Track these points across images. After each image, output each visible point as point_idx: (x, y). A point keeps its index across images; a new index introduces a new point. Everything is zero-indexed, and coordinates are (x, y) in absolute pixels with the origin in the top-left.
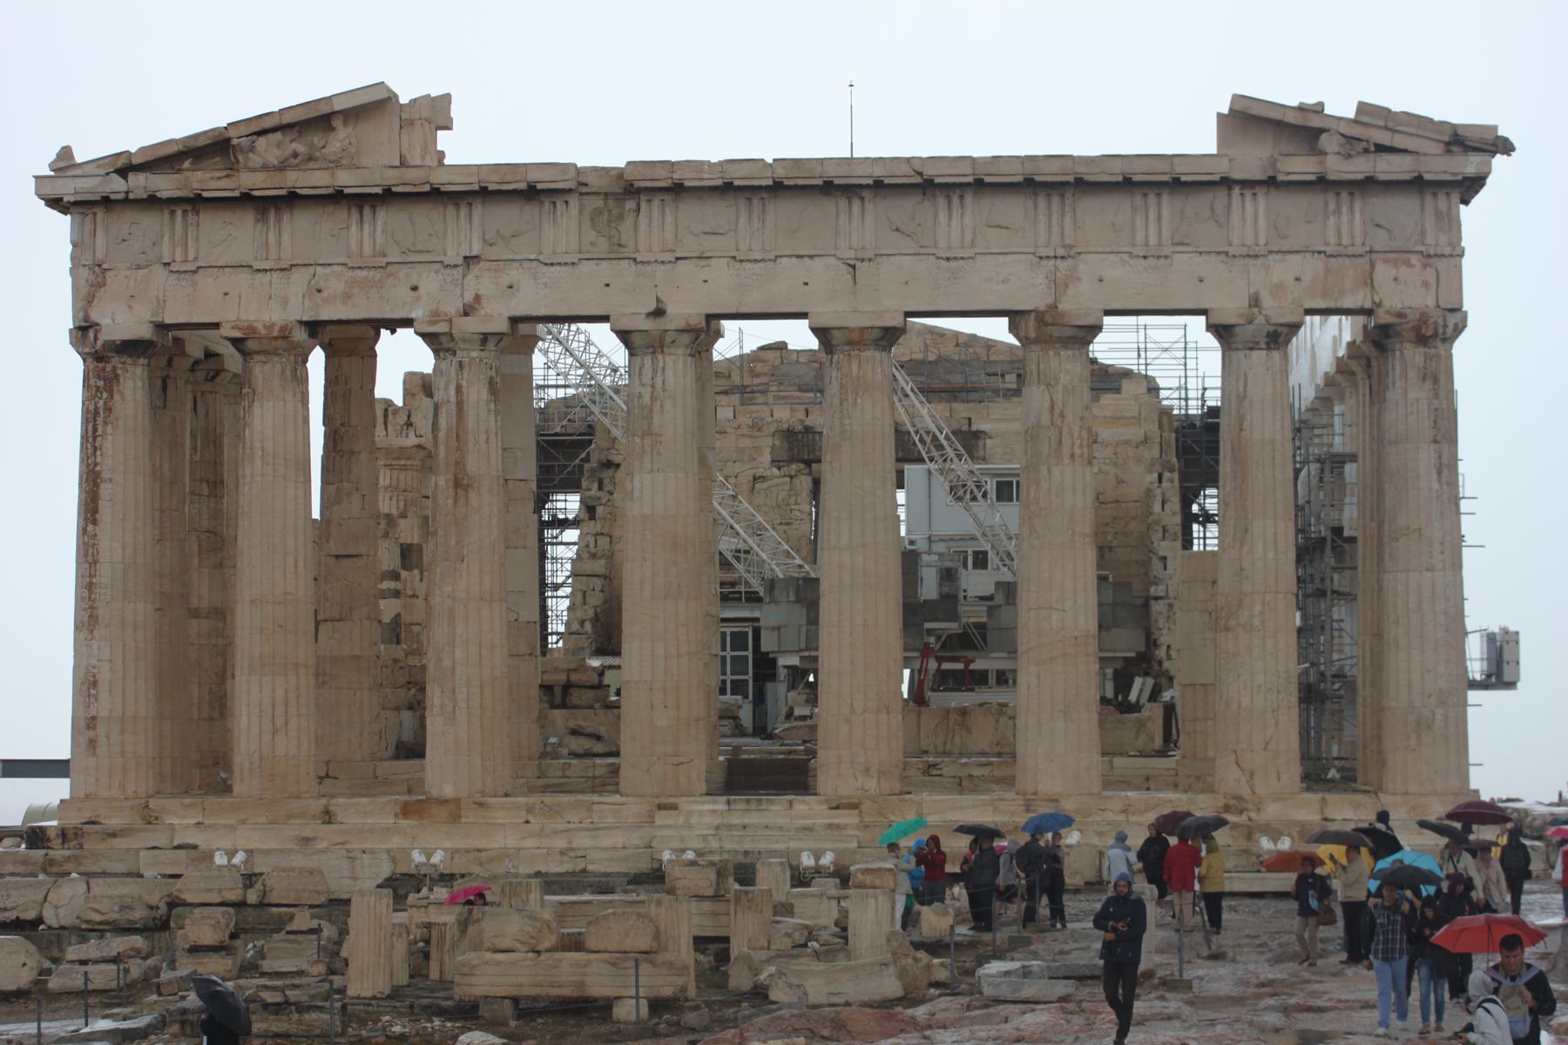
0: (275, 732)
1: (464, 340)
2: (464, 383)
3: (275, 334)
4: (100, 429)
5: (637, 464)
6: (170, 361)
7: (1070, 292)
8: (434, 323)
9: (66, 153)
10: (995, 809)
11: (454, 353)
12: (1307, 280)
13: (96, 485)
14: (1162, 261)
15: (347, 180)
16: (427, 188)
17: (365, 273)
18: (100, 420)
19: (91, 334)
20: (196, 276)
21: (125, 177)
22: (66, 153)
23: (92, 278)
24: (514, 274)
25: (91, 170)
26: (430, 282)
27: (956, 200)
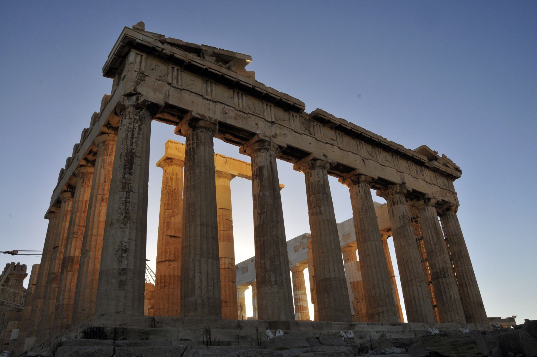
1: (273, 146)
3: (213, 121)
4: (136, 135)
5: (322, 203)
8: (265, 137)
9: (142, 24)
11: (268, 151)
13: (133, 158)
15: (242, 79)
17: (241, 113)
18: (136, 132)
19: (134, 98)
20: (182, 92)
21: (163, 44)
22: (142, 24)
23: (138, 77)
24: (285, 131)
25: (150, 35)
26: (262, 124)
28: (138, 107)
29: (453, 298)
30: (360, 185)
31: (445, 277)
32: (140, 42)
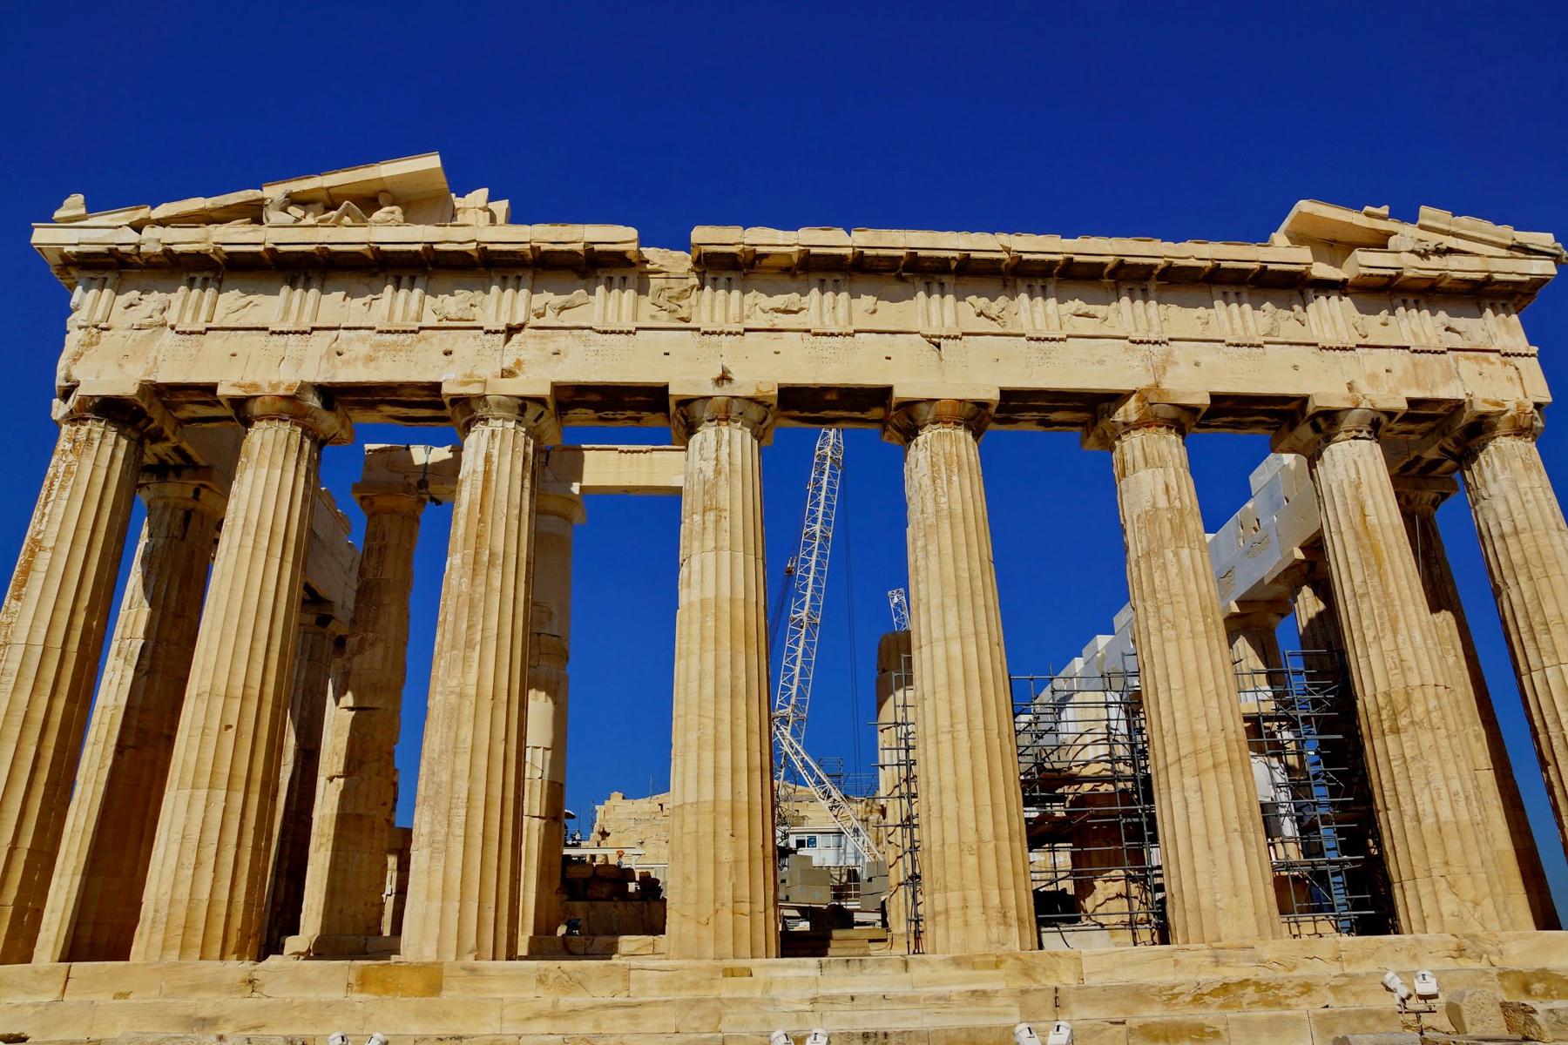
0: (198, 864)
2: (495, 452)
3: (281, 392)
4: (54, 493)
5: (696, 544)
6: (197, 492)
7: (1169, 374)
8: (467, 384)
10: (1177, 962)
12: (1398, 371)
14: (1254, 350)
16: (473, 246)
17: (395, 337)
24: (562, 340)
26: (464, 343)
27: (1038, 289)
28: (75, 418)
29: (1428, 821)
30: (920, 439)
31: (1396, 731)
32: (74, 249)
